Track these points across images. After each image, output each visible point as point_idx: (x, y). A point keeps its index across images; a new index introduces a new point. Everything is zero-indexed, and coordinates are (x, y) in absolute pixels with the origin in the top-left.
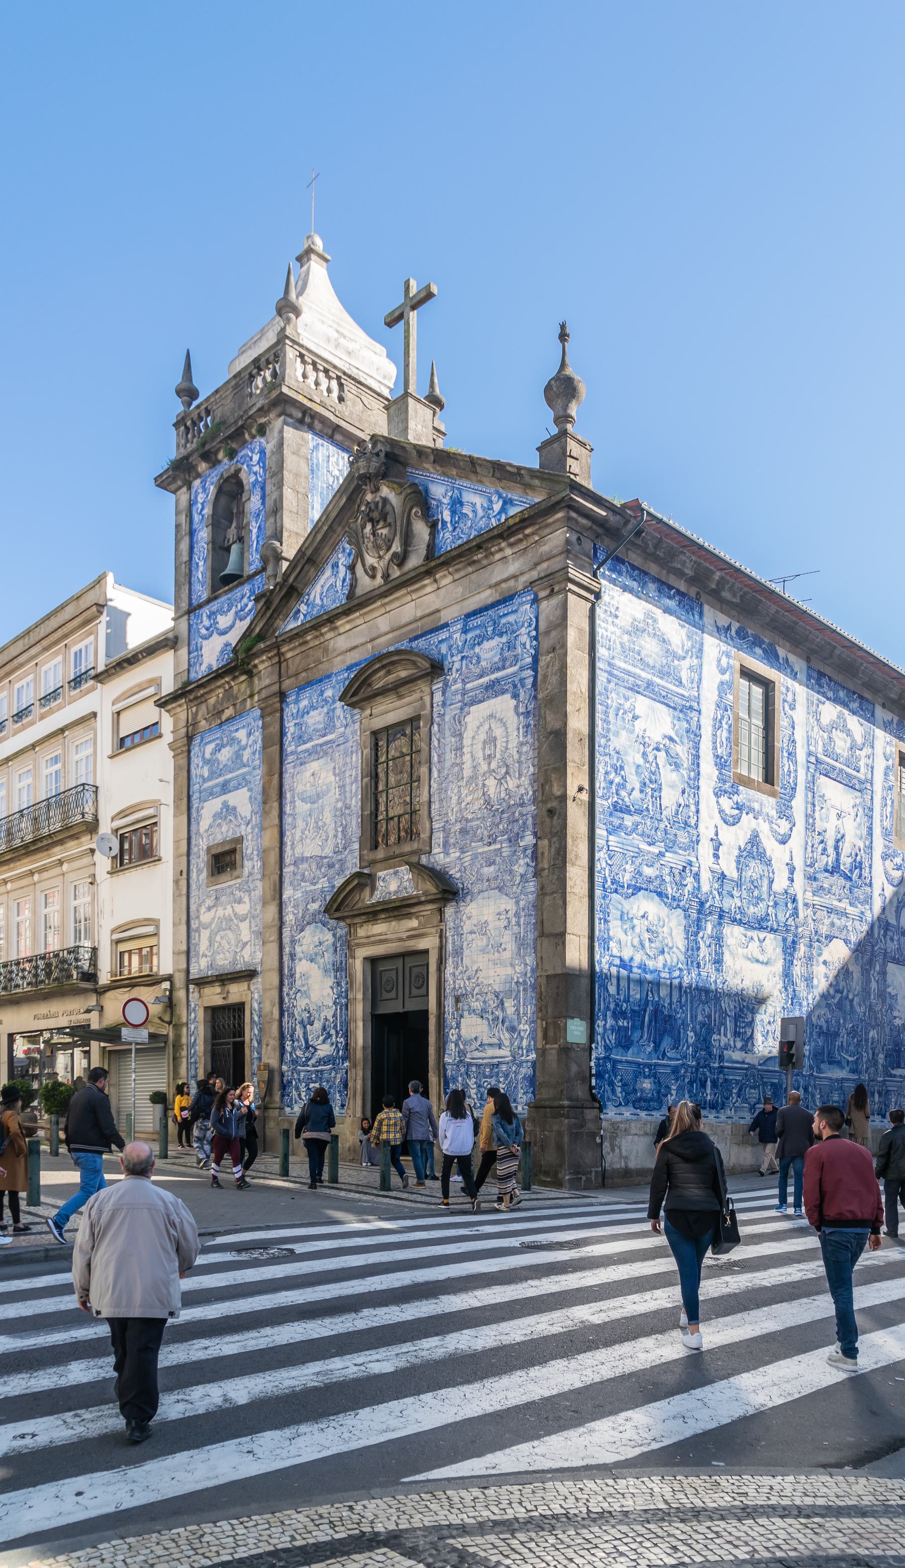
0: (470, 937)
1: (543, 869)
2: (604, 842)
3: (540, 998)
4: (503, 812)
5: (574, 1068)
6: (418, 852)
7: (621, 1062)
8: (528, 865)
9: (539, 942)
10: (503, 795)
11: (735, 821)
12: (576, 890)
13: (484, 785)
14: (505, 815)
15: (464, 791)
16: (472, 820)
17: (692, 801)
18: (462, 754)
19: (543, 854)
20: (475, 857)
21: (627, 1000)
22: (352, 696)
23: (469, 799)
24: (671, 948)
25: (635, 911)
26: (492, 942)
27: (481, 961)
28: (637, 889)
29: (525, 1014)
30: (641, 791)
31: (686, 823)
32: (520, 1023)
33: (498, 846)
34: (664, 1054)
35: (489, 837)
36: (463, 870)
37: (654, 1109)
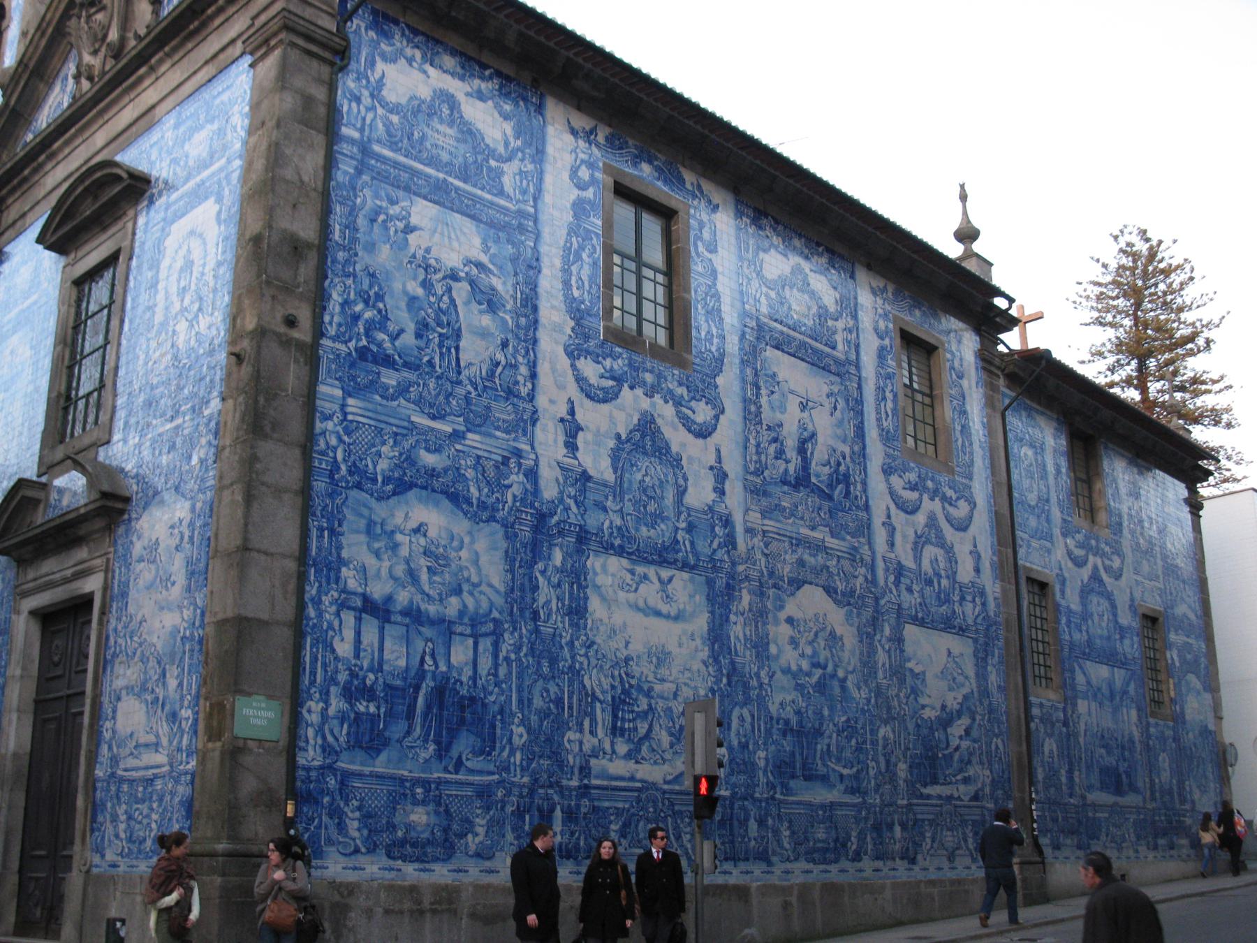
1: (224, 448)
2: (336, 407)
5: (249, 785)
6: (97, 445)
7: (360, 775)
10: (193, 342)
11: (607, 397)
12: (265, 479)
13: (174, 331)
15: (153, 344)
17: (520, 359)
18: (157, 292)
20: (154, 441)
21: (378, 668)
23: (157, 354)
24: (476, 586)
25: (399, 519)
26: (161, 572)
28: (401, 486)
30: (418, 336)
31: (510, 393)
32: (181, 708)
34: (459, 764)
37: (436, 860)
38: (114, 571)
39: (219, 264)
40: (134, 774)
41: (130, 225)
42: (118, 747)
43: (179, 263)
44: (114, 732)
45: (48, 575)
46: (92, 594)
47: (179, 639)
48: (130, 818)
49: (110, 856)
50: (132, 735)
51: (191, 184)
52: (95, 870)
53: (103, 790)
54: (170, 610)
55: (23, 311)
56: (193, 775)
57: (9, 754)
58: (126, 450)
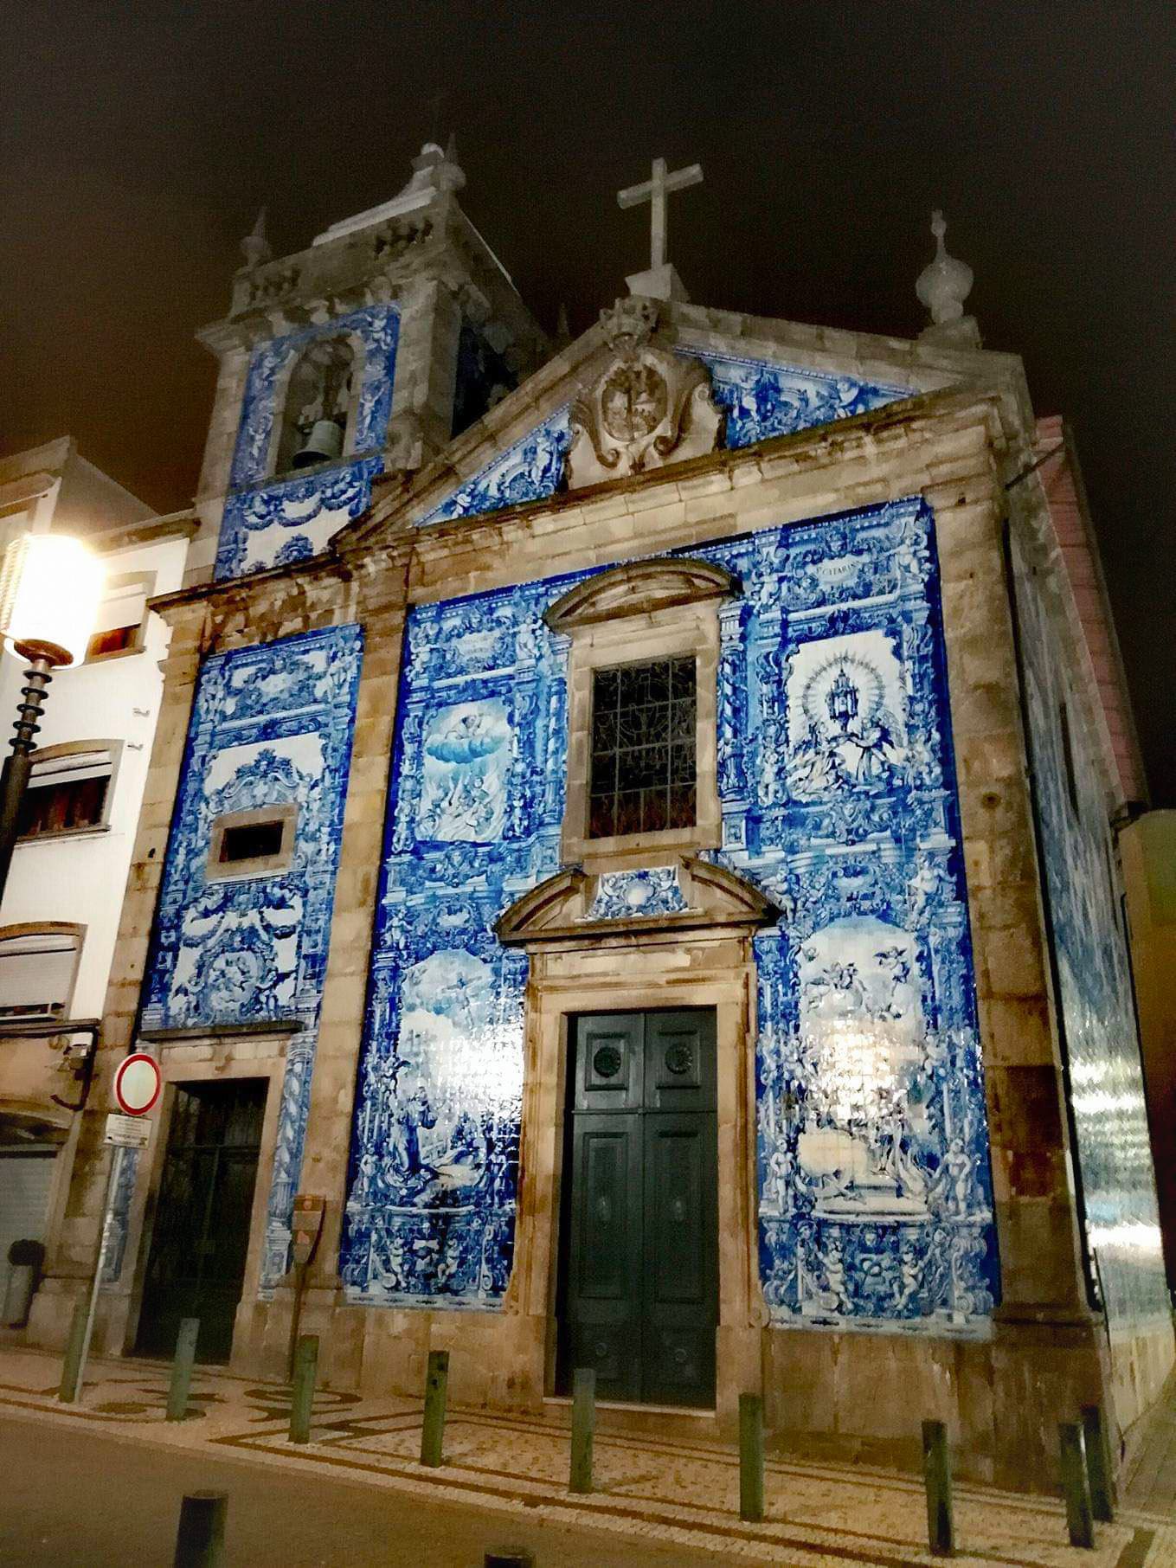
0: (816, 990)
3: (997, 1106)
4: (877, 796)
8: (940, 879)
9: (982, 1007)
10: (876, 769)
13: (832, 754)
14: (879, 802)
16: (807, 805)
19: (976, 863)
20: (819, 860)
22: (565, 614)
23: (803, 773)
32: (945, 1151)
33: (873, 847)
35: (849, 832)
39: (912, 699)
43: (826, 685)
45: (605, 974)
46: (711, 1009)
48: (850, 1268)
49: (810, 1310)
50: (837, 1174)
51: (828, 610)
52: (778, 1325)
55: (485, 682)
56: (990, 1233)
58: (757, 862)
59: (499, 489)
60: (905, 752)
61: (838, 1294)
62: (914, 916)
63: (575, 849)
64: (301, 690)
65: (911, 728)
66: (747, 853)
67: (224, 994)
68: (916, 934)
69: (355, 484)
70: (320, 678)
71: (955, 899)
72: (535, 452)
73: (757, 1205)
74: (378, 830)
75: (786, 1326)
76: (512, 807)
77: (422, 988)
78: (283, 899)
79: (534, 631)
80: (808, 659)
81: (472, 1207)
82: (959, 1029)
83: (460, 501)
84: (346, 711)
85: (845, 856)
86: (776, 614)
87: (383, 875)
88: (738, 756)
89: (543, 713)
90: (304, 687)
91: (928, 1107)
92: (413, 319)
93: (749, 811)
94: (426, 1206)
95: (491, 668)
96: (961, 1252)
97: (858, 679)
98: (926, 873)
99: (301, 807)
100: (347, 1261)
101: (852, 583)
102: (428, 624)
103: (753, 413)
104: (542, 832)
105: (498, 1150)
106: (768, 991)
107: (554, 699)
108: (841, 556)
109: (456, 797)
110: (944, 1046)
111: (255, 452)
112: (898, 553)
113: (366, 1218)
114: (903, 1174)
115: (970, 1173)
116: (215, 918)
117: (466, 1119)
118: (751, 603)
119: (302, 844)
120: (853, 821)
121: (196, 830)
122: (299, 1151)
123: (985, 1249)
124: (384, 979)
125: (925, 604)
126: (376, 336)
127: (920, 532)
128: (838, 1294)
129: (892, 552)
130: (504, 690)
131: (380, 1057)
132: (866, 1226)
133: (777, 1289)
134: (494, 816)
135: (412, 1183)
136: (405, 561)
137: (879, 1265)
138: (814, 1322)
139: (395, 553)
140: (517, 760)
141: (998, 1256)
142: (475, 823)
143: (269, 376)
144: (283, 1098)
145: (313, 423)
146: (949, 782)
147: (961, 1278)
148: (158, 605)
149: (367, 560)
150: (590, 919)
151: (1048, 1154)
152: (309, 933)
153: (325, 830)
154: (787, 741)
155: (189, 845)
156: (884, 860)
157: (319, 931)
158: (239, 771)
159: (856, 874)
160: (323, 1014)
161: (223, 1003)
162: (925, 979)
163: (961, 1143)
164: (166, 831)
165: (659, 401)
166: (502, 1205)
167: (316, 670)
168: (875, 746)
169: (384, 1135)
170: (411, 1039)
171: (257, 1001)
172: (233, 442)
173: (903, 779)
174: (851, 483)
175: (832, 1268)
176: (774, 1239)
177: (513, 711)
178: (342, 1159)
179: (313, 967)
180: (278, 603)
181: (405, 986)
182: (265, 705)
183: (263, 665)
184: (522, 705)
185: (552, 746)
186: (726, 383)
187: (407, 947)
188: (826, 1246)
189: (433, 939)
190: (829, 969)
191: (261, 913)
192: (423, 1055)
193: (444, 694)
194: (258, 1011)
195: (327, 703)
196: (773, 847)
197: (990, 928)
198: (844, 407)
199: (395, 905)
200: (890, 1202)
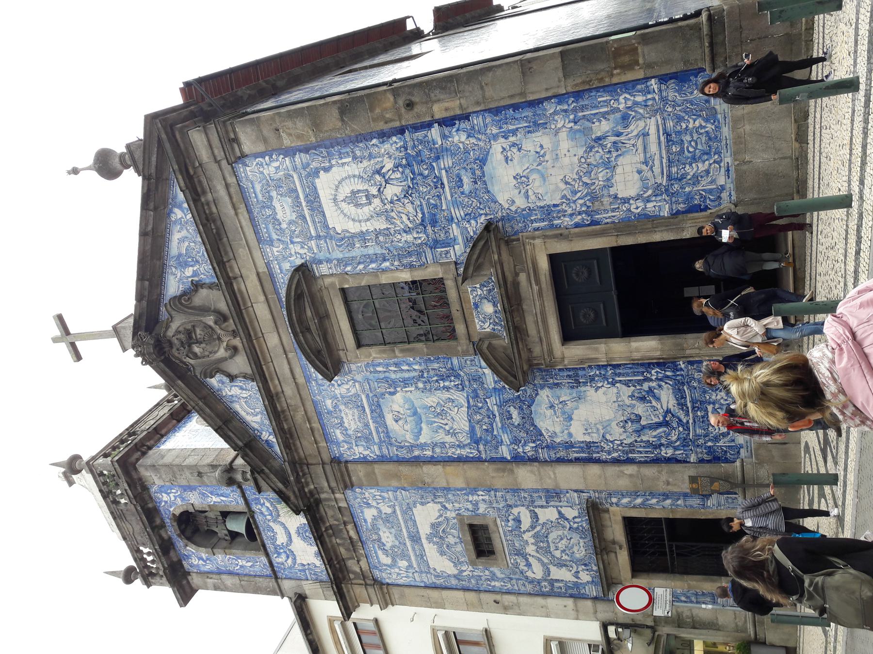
0: (532, 198)
1: (461, 106)
4: (413, 173)
8: (458, 130)
9: (531, 98)
10: (399, 175)
14: (416, 171)
19: (446, 109)
20: (456, 204)
22: (327, 369)
23: (405, 218)
26: (534, 167)
27: (556, 177)
29: (607, 102)
32: (619, 108)
33: (443, 172)
36: (468, 217)
38: (534, 229)
39: (355, 158)
40: (664, 161)
41: (328, 281)
42: (648, 188)
43: (350, 209)
44: (638, 197)
47: (576, 127)
48: (694, 159)
49: (721, 181)
50: (639, 172)
51: (307, 212)
53: (677, 202)
54: (558, 145)
55: (372, 411)
57: (660, 347)
59: (256, 415)
60: (386, 160)
61: (710, 164)
62: (481, 144)
63: (465, 348)
64: (388, 521)
65: (371, 157)
66: (455, 246)
67: (575, 549)
68: (492, 141)
69: (262, 502)
70: (380, 511)
71: (469, 120)
72: (232, 396)
73: (663, 217)
74: (466, 466)
75: (733, 193)
76: (444, 387)
77: (558, 430)
78: (514, 520)
79: (339, 385)
80: (337, 222)
81: (685, 388)
82: (546, 109)
83: (265, 438)
84: (398, 493)
85: (450, 189)
86: (313, 243)
87: (492, 460)
88: (400, 257)
89: (387, 374)
90: (388, 520)
91: (594, 123)
92: (160, 477)
93: (431, 248)
94: (688, 415)
95: (363, 407)
96: (677, 94)
97: (345, 190)
98: (456, 139)
99: (458, 515)
100: (726, 458)
101: (290, 200)
102: (341, 449)
103: (195, 268)
104: (457, 367)
105: (649, 375)
106: (536, 225)
107: (379, 369)
108: (274, 209)
109: (442, 422)
110: (556, 117)
111: (250, 564)
112: (269, 174)
113: (699, 450)
114: (635, 133)
115: (629, 94)
116: (531, 559)
117: (632, 396)
118: (308, 258)
119: (481, 511)
120: (430, 185)
121: (480, 576)
122: (664, 494)
123: (673, 81)
124: (555, 454)
125: (297, 156)
126: (173, 499)
127: (255, 163)
128: (710, 164)
129: (268, 178)
130: (376, 399)
131: (602, 451)
132: (668, 151)
133: (711, 200)
134: (451, 397)
135: (675, 425)
136: (305, 467)
137: (690, 142)
138: (729, 177)
139: (301, 474)
140: (416, 387)
141: (676, 73)
142: (456, 408)
143: (205, 561)
144: (634, 507)
145: (229, 531)
146: (401, 131)
147: (692, 93)
148: (347, 612)
149: (306, 490)
150: (505, 334)
151: (613, 49)
152: (533, 502)
153: (471, 498)
154: (388, 229)
155: (488, 580)
156: (451, 165)
157: (531, 496)
158: (441, 555)
159: (461, 180)
160: (581, 487)
161: (581, 548)
162: (518, 134)
163: (613, 101)
164: (483, 596)
165: (194, 326)
166: (681, 369)
167: (374, 512)
168: (384, 177)
169: (648, 444)
170: (589, 433)
171: (577, 528)
172: (246, 579)
173: (402, 159)
174: (230, 206)
175: (695, 169)
176: (682, 206)
177: (387, 392)
178: (665, 468)
179: (553, 497)
180: (338, 541)
181: (558, 440)
182: (400, 543)
183: (376, 546)
184: (382, 388)
185: (405, 368)
186: (179, 287)
187: (534, 442)
188: (683, 174)
189: (527, 426)
190: (517, 191)
191: (524, 532)
192: (598, 426)
193: (382, 435)
194: (583, 528)
195: (395, 506)
196: (451, 231)
197: (484, 97)
198: (186, 216)
199: (510, 451)
200: (653, 137)
